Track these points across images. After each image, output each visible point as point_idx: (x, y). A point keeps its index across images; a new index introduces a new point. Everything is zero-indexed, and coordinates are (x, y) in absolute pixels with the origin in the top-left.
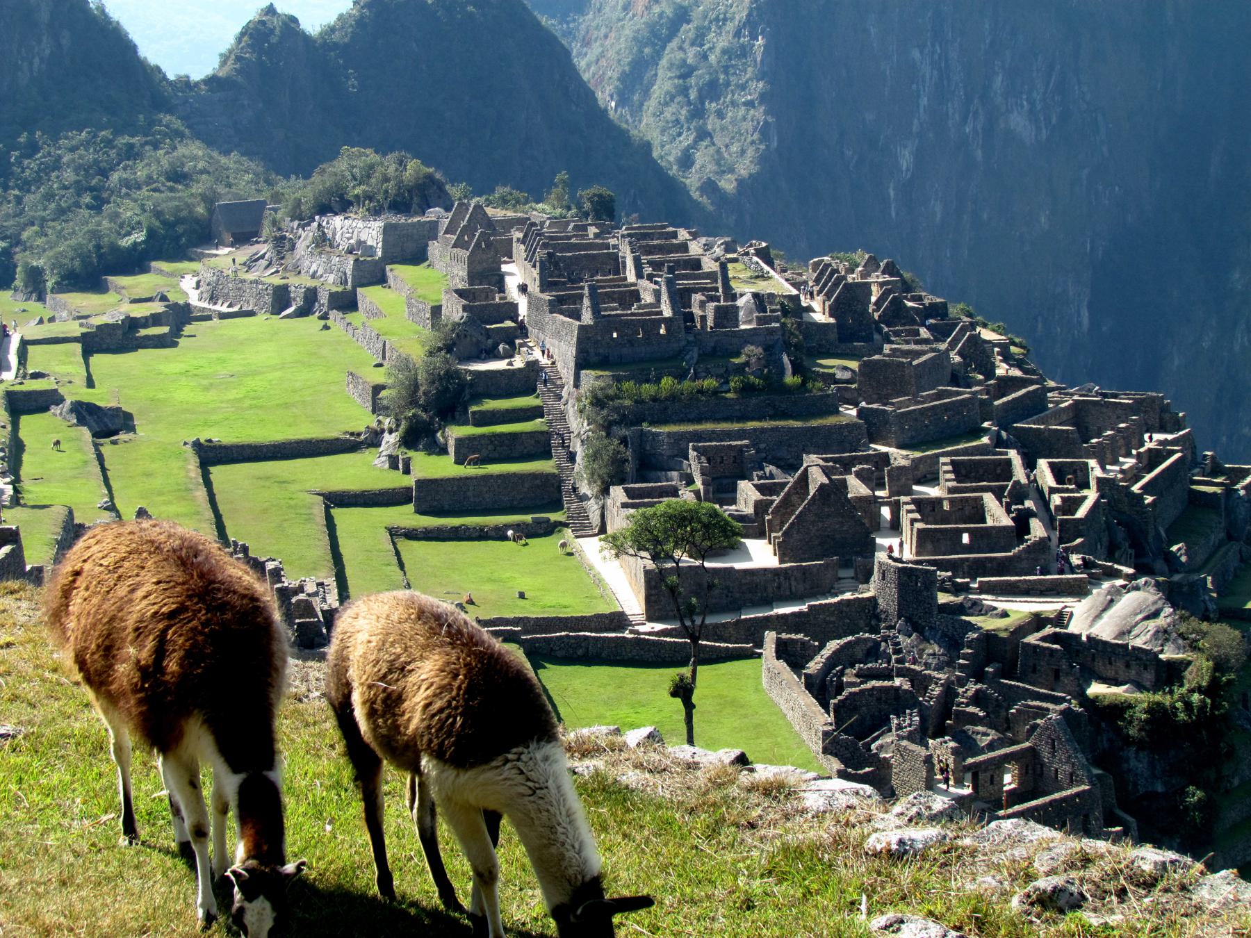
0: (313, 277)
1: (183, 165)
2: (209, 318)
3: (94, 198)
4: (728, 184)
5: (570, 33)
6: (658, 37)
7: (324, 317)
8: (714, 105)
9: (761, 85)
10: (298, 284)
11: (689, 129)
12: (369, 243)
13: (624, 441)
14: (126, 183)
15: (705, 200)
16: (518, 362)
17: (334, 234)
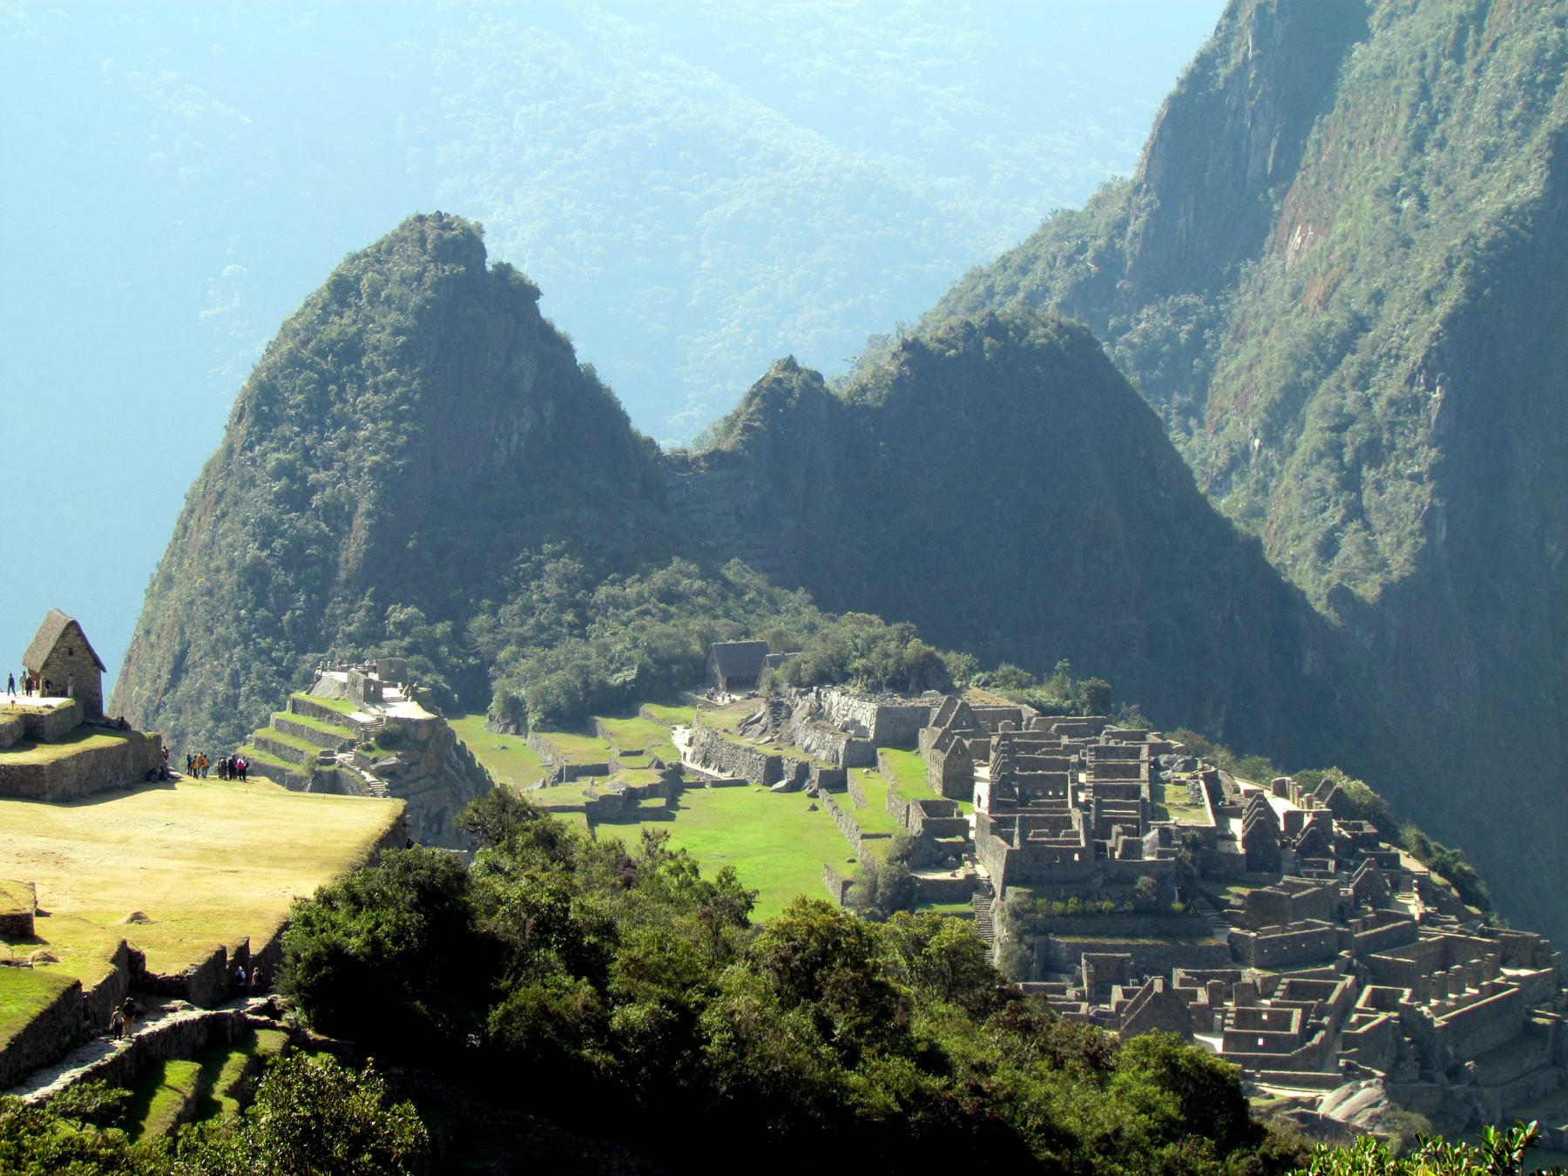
0: (806, 750)
1: (678, 583)
2: (700, 785)
3: (576, 616)
4: (1368, 590)
5: (1220, 318)
6: (1325, 354)
7: (814, 795)
8: (1372, 473)
9: (1434, 452)
10: (792, 757)
11: (1336, 503)
12: (863, 723)
13: (1031, 947)
14: (613, 601)
15: (1331, 615)
16: (961, 874)
17: (831, 708)
